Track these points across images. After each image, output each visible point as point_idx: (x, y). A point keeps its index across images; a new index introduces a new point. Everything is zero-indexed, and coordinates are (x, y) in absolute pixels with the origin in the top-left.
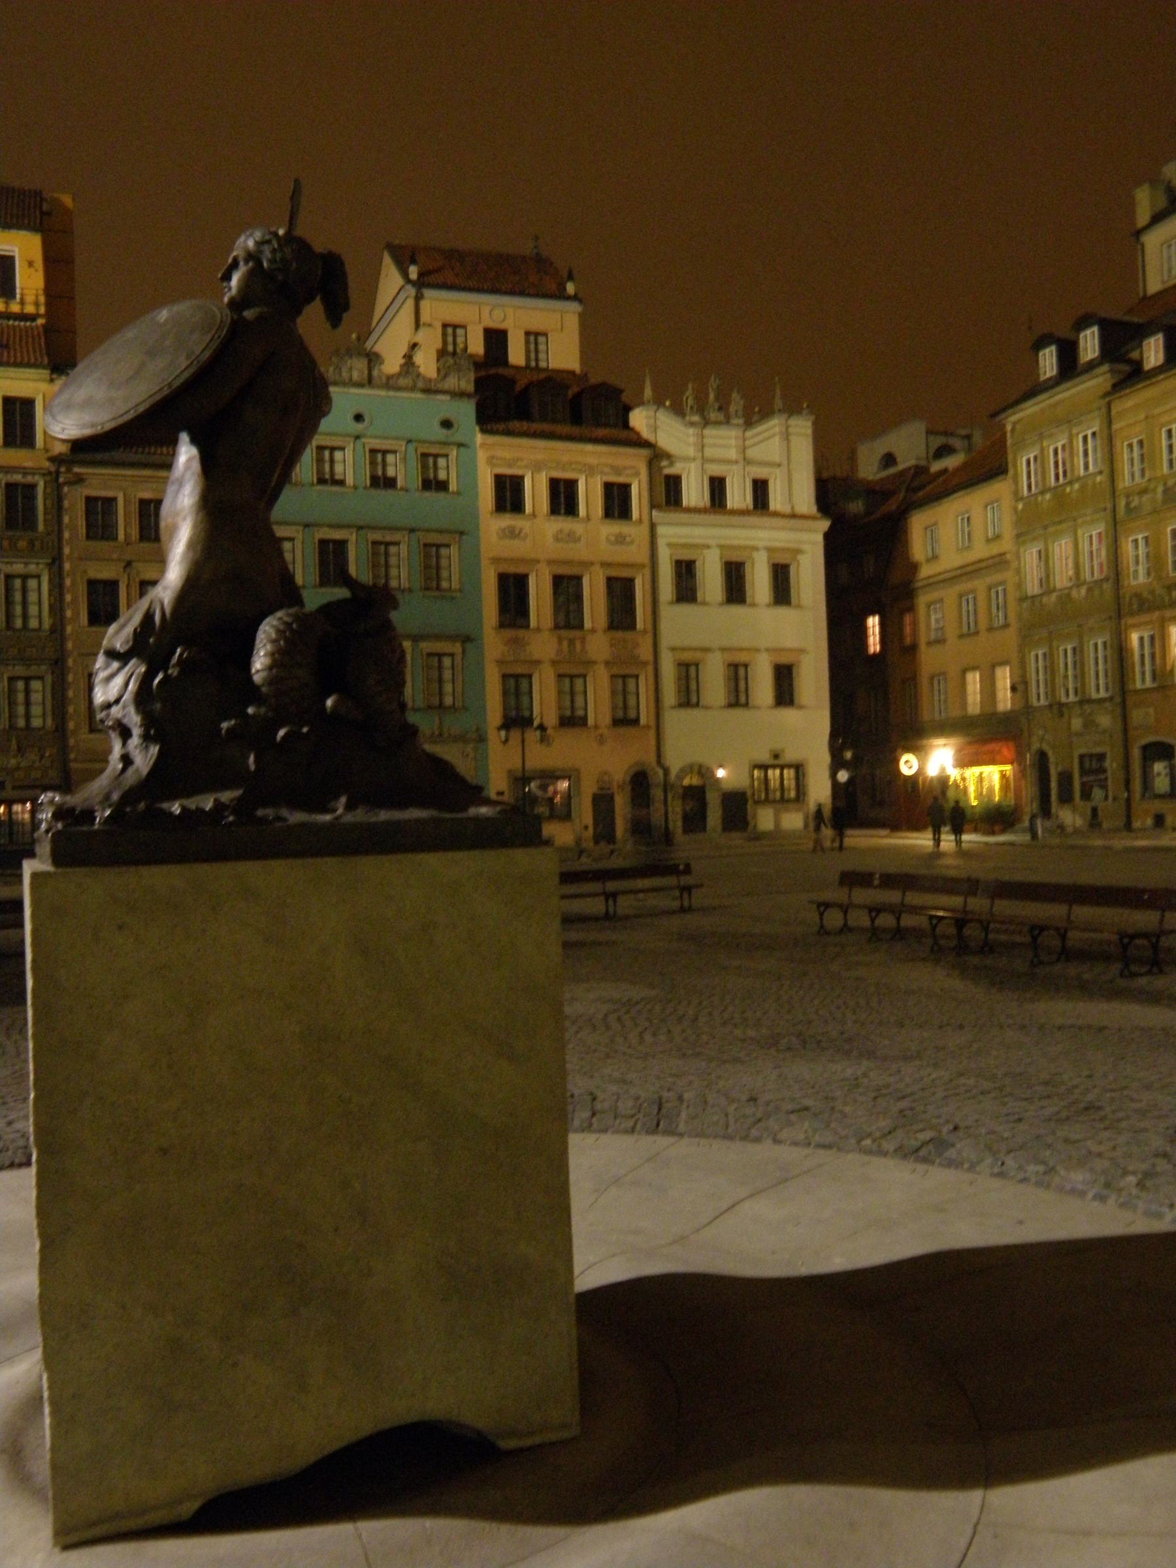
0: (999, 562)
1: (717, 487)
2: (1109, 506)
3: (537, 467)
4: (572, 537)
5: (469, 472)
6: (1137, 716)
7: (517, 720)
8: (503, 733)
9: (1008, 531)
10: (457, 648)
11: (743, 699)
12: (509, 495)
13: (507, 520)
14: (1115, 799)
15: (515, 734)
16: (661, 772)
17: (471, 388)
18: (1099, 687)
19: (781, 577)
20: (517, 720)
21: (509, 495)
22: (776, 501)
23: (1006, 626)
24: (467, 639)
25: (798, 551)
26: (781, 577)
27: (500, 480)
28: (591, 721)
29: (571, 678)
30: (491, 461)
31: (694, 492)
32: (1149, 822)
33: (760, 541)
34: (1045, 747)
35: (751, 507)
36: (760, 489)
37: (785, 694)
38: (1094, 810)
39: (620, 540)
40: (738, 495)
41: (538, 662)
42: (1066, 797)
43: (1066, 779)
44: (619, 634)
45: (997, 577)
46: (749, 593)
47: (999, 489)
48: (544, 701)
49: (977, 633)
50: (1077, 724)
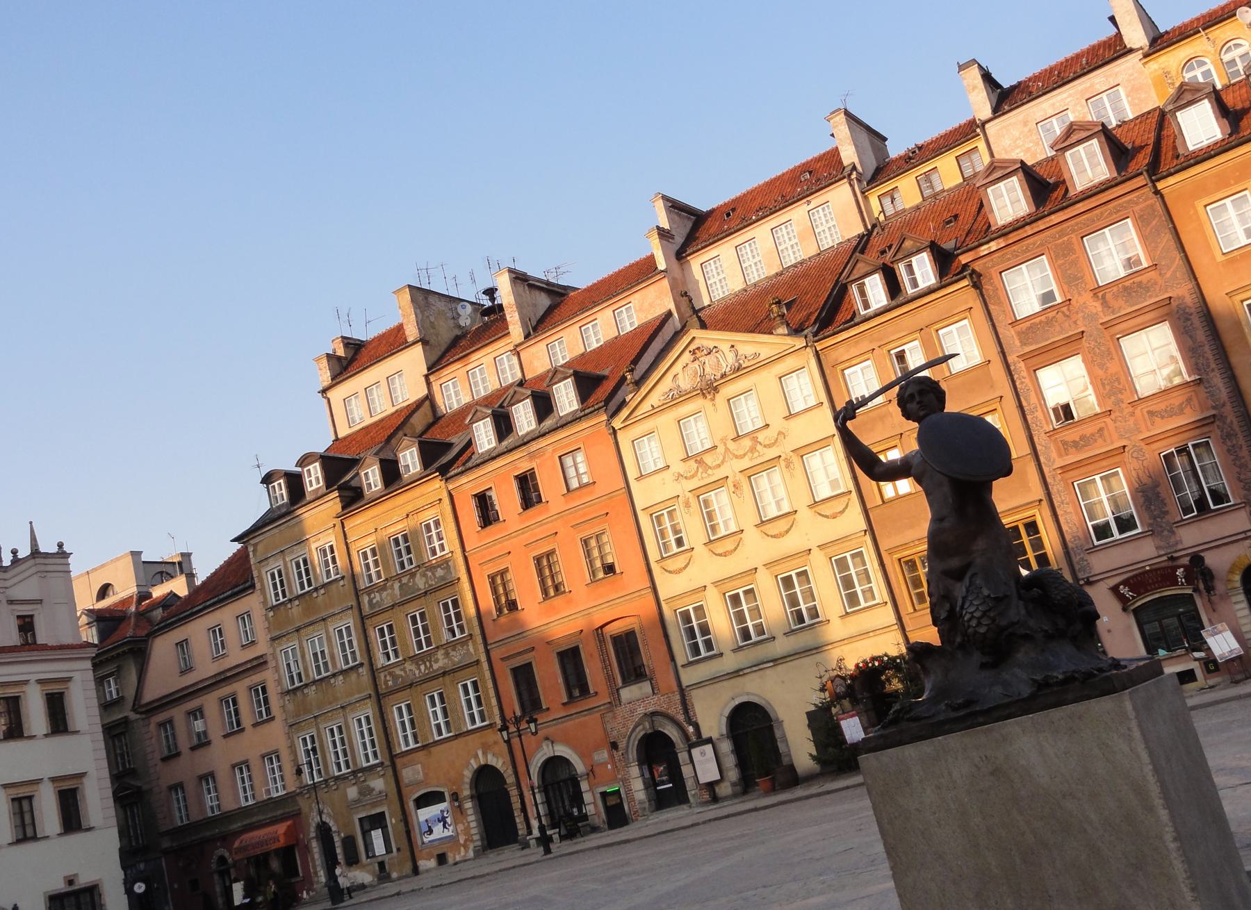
0: (259, 664)
2: (354, 603)
6: (407, 774)
9: (262, 637)
11: (29, 833)
14: (398, 850)
18: (365, 755)
19: (57, 708)
22: (42, 637)
23: (273, 719)
25: (69, 679)
26: (57, 708)
32: (432, 863)
37: (72, 820)
38: (382, 865)
42: (353, 860)
43: (349, 842)
45: (256, 678)
46: (25, 726)
47: (251, 603)
49: (243, 730)
50: (352, 792)
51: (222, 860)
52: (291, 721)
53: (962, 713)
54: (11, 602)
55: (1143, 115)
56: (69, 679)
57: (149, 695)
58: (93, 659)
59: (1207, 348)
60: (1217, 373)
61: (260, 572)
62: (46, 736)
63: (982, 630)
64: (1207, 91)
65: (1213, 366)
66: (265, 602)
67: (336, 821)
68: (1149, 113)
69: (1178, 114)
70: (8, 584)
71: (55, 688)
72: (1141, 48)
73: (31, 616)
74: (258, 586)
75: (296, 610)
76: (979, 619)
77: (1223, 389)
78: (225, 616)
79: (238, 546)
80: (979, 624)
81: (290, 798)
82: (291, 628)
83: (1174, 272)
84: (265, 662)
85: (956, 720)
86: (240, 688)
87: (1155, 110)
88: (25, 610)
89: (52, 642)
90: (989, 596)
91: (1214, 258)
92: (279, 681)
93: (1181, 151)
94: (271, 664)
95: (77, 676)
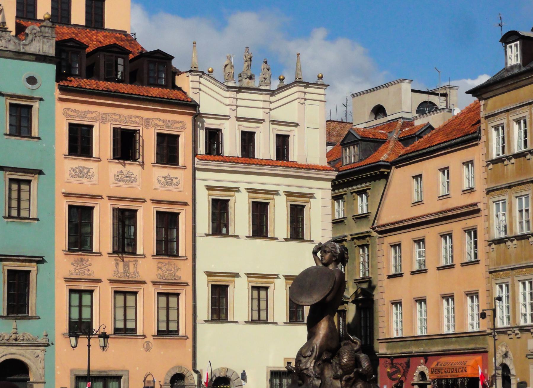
0: (473, 211)
1: (248, 139)
3: (104, 120)
4: (130, 178)
5: (51, 122)
7: (79, 328)
8: (73, 339)
9: (480, 188)
10: (32, 267)
12: (80, 141)
13: (77, 162)
15: (83, 341)
16: (195, 376)
17: (52, 52)
20: (79, 328)
21: (80, 141)
22: (294, 155)
24: (41, 261)
25: (311, 196)
27: (73, 128)
28: (139, 332)
29: (125, 293)
30: (65, 113)
31: (231, 146)
33: (279, 186)
34: (507, 362)
35: (274, 157)
36: (282, 143)
39: (169, 181)
40: (265, 148)
41: (99, 281)
44: (165, 260)
45: (469, 222)
46: (270, 228)
47: (473, 153)
48: (103, 313)
49: (452, 266)
51: (422, 374)
52: (492, 268)
54: (273, 122)
56: (311, 196)
57: (387, 217)
58: (333, 181)
61: (487, 127)
62: (286, 240)
66: (487, 154)
67: (515, 365)
70: (273, 106)
71: (298, 201)
73: (288, 136)
74: (483, 138)
75: (510, 167)
78: (454, 160)
79: (472, 100)
81: (481, 334)
82: (504, 183)
84: (478, 211)
86: (456, 227)
88: (283, 130)
89: (301, 161)
92: (488, 230)
94: (483, 213)
95: (318, 194)
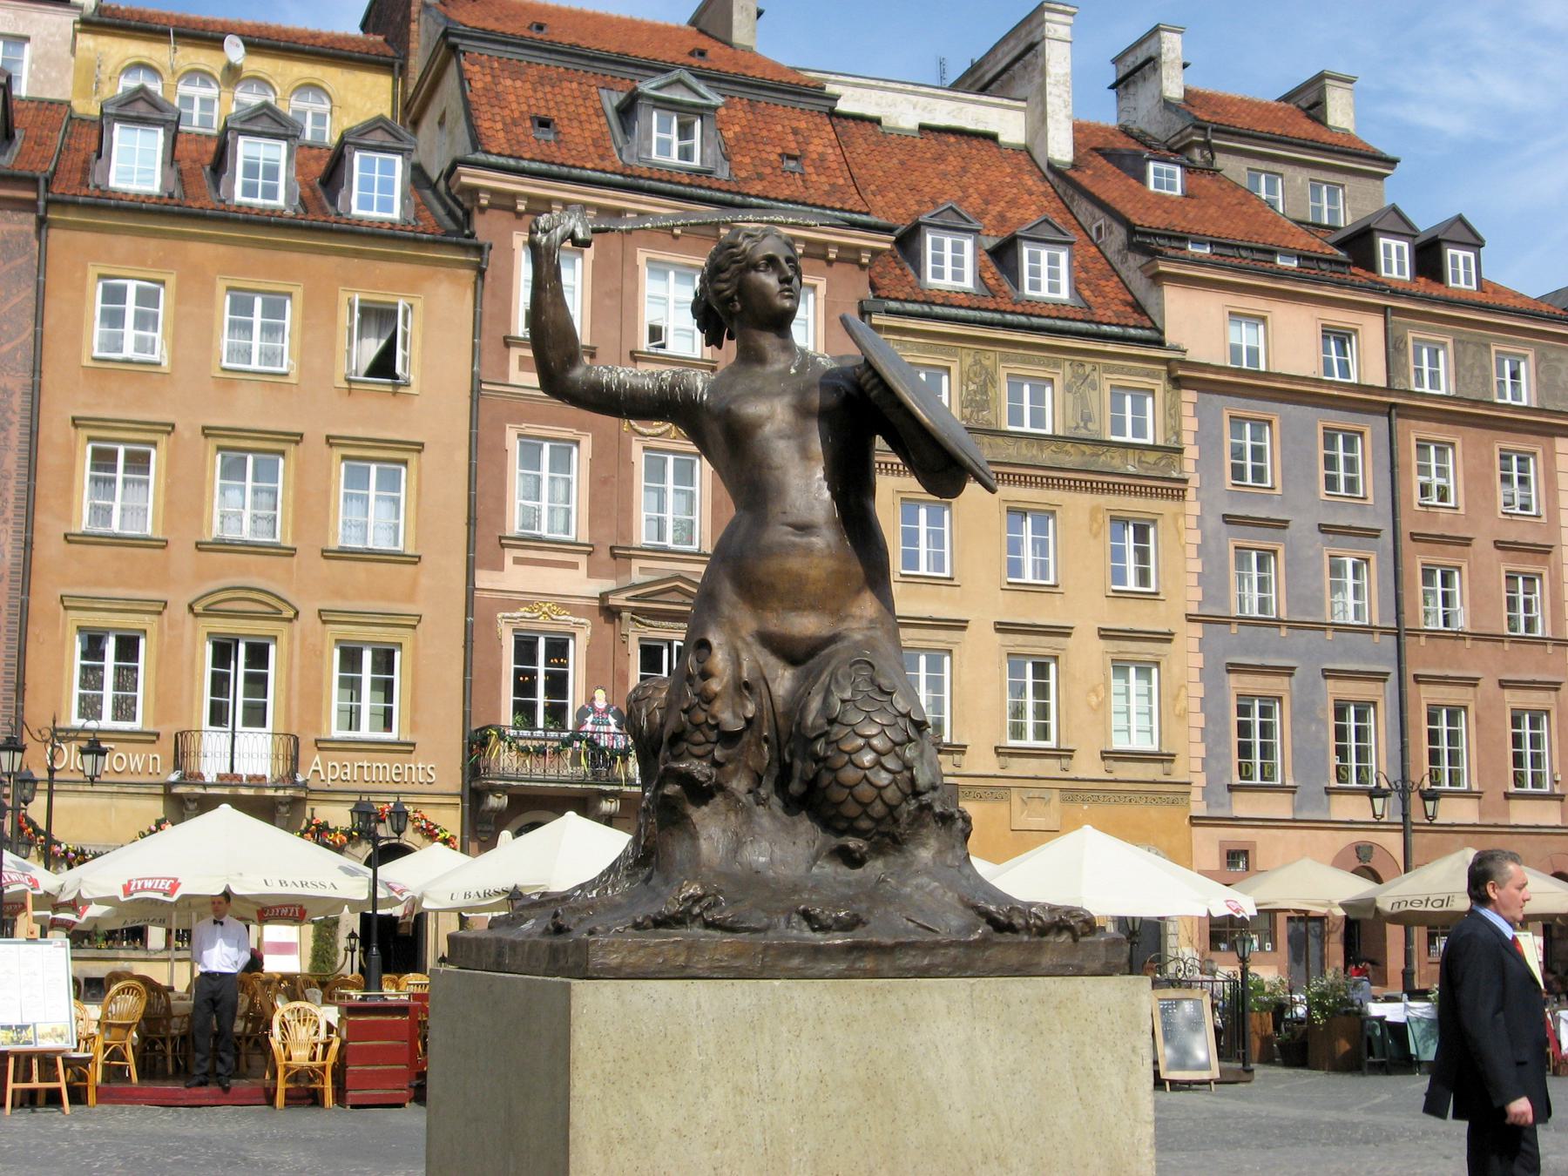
53: (838, 940)
55: (41, 101)
59: (12, 484)
60: (9, 527)
63: (883, 778)
64: (169, 116)
65: (9, 514)
68: (51, 103)
69: (117, 126)
72: (80, 7)
76: (879, 753)
77: (8, 556)
80: (878, 764)
83: (15, 349)
85: (817, 952)
87: (61, 103)
90: (903, 715)
91: (79, 356)
93: (98, 179)
